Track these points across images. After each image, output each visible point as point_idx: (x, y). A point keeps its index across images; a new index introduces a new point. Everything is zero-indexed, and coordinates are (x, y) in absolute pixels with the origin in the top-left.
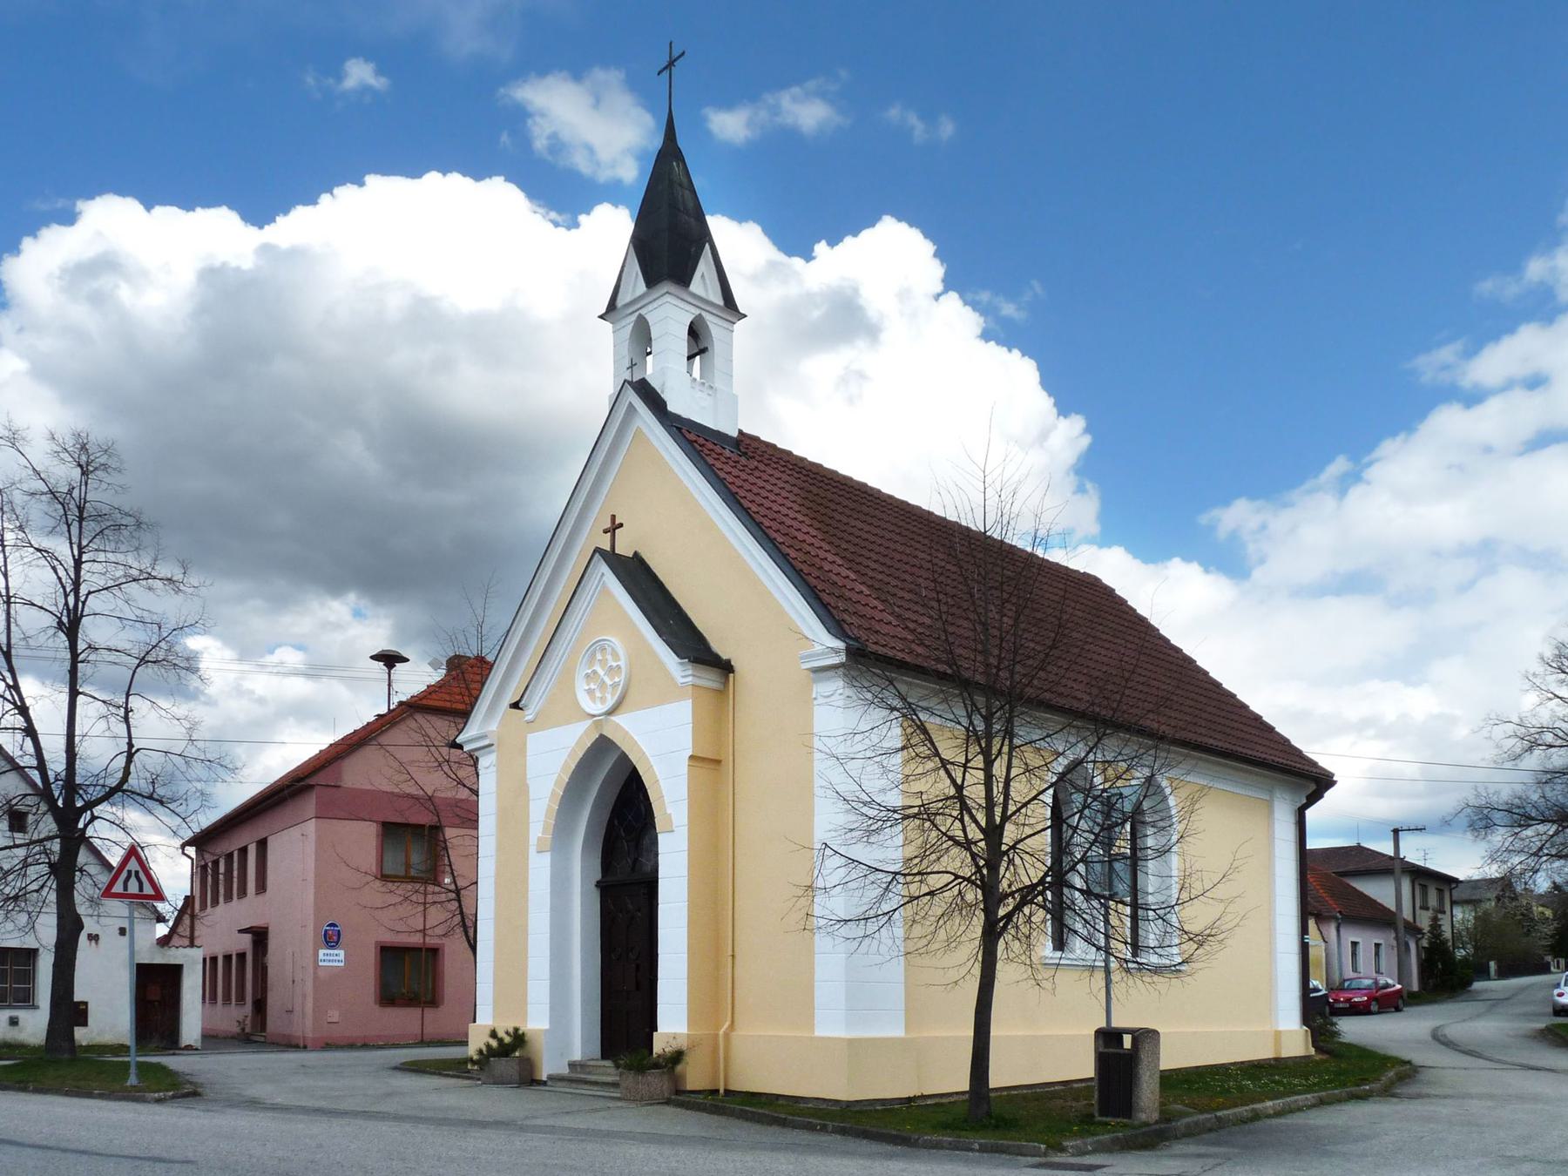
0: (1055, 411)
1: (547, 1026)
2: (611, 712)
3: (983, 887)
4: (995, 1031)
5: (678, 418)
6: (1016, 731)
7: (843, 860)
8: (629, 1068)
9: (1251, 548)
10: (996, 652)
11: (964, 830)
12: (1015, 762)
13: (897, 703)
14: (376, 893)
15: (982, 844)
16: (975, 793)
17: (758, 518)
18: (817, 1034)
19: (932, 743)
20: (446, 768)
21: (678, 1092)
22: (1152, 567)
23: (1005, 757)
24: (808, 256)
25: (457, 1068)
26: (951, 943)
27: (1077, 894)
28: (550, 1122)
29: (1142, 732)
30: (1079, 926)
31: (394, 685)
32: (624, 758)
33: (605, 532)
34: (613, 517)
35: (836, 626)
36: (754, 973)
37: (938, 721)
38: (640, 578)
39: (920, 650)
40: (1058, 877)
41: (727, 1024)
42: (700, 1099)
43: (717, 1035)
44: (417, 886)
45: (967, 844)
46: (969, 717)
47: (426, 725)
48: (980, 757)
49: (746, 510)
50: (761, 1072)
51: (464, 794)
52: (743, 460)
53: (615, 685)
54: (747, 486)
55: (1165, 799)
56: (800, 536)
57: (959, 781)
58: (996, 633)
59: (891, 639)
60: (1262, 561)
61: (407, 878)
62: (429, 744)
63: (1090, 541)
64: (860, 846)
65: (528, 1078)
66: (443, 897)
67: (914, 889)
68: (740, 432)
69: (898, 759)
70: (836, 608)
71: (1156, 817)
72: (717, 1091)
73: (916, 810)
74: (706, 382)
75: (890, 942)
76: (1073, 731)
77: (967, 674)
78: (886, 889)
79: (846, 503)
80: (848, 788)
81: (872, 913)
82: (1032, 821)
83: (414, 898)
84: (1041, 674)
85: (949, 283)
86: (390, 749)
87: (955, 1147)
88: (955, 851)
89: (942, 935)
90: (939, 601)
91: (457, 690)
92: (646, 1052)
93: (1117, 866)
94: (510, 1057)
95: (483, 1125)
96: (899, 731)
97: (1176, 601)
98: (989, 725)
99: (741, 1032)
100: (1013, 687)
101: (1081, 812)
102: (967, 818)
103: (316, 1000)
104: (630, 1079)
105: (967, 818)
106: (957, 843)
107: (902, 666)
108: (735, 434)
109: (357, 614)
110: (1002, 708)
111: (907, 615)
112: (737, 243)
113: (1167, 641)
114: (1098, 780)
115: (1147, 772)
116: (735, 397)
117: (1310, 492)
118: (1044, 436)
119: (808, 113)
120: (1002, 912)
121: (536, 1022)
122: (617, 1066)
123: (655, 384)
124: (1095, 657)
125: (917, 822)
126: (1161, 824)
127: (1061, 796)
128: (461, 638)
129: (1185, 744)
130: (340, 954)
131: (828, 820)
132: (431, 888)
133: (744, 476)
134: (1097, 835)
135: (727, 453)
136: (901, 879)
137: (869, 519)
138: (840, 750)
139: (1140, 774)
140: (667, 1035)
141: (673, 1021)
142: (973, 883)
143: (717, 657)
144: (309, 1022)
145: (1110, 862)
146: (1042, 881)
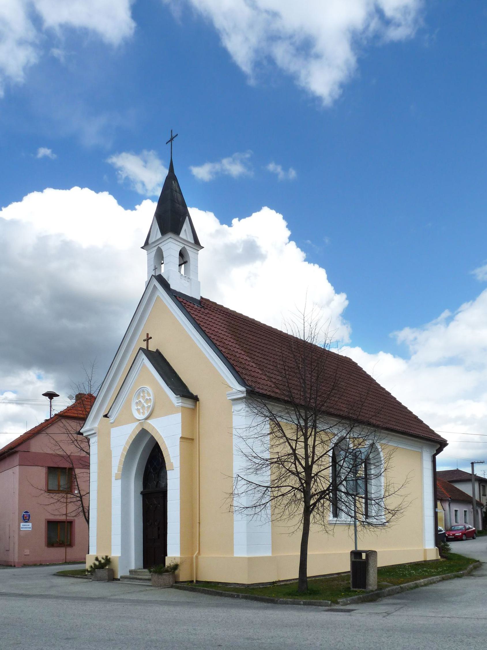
0: (334, 292)
1: (120, 555)
2: (147, 419)
3: (304, 492)
4: (309, 553)
5: (175, 291)
6: (317, 425)
7: (245, 482)
8: (155, 572)
9: (411, 348)
10: (309, 391)
11: (296, 468)
12: (317, 439)
13: (268, 414)
14: (46, 498)
15: (304, 474)
16: (300, 452)
17: (209, 335)
18: (235, 555)
19: (282, 430)
20: (76, 443)
21: (176, 582)
22: (372, 356)
23: (313, 437)
24: (230, 225)
25: (81, 574)
26: (291, 515)
27: (343, 494)
28: (122, 597)
29: (369, 424)
30: (343, 508)
31: (53, 407)
32: (152, 438)
33: (144, 341)
34: (148, 334)
35: (242, 381)
36: (208, 528)
37: (285, 421)
38: (158, 360)
39: (277, 391)
40: (335, 487)
41: (197, 552)
42: (185, 585)
43: (192, 557)
44: (64, 494)
45: (297, 474)
46: (298, 420)
47: (67, 425)
48: (303, 437)
49: (204, 331)
50: (211, 572)
51: (84, 454)
52: (203, 310)
53: (149, 407)
54: (204, 321)
55: (379, 454)
56: (227, 342)
57: (294, 447)
58: (310, 383)
59: (265, 386)
60: (415, 353)
61: (58, 491)
62: (68, 433)
63: (347, 345)
64: (253, 475)
65: (112, 578)
66: (75, 500)
67: (275, 494)
68: (201, 298)
69: (268, 438)
70: (242, 373)
71: (375, 461)
72: (193, 581)
73: (276, 460)
74: (187, 276)
75: (265, 516)
76: (341, 425)
77: (297, 401)
78: (264, 493)
79: (246, 328)
80: (247, 451)
81: (258, 504)
82: (324, 463)
83: (62, 500)
84: (328, 401)
85: (291, 239)
86: (51, 435)
87: (293, 603)
88: (292, 476)
89: (287, 512)
90: (285, 370)
91: (80, 409)
92: (162, 565)
93: (359, 482)
94: (104, 569)
95: (92, 599)
96: (268, 426)
97: (382, 369)
98: (306, 423)
99: (202, 555)
100: (316, 406)
101: (344, 459)
102: (297, 463)
103: (19, 545)
104: (155, 577)
105: (297, 463)
106: (293, 473)
107: (269, 398)
108: (199, 298)
109: (39, 377)
110: (312, 415)
111: (272, 375)
112: (202, 220)
113: (379, 385)
114: (351, 446)
115: (371, 442)
116: (199, 282)
117: (436, 324)
118: (329, 302)
119: (235, 169)
120: (312, 502)
121: (115, 553)
122: (150, 572)
123: (165, 277)
124: (350, 393)
125: (277, 465)
126: (377, 464)
127: (336, 453)
128: (82, 387)
129: (387, 429)
130: (30, 525)
131: (239, 464)
132: (69, 496)
133: (203, 316)
134: (351, 469)
135: (196, 307)
136: (270, 489)
137: (256, 335)
138: (244, 435)
139: (368, 443)
140: (171, 558)
141: (174, 552)
142: (300, 490)
143: (192, 394)
144: (16, 555)
145: (356, 480)
146: (328, 489)
